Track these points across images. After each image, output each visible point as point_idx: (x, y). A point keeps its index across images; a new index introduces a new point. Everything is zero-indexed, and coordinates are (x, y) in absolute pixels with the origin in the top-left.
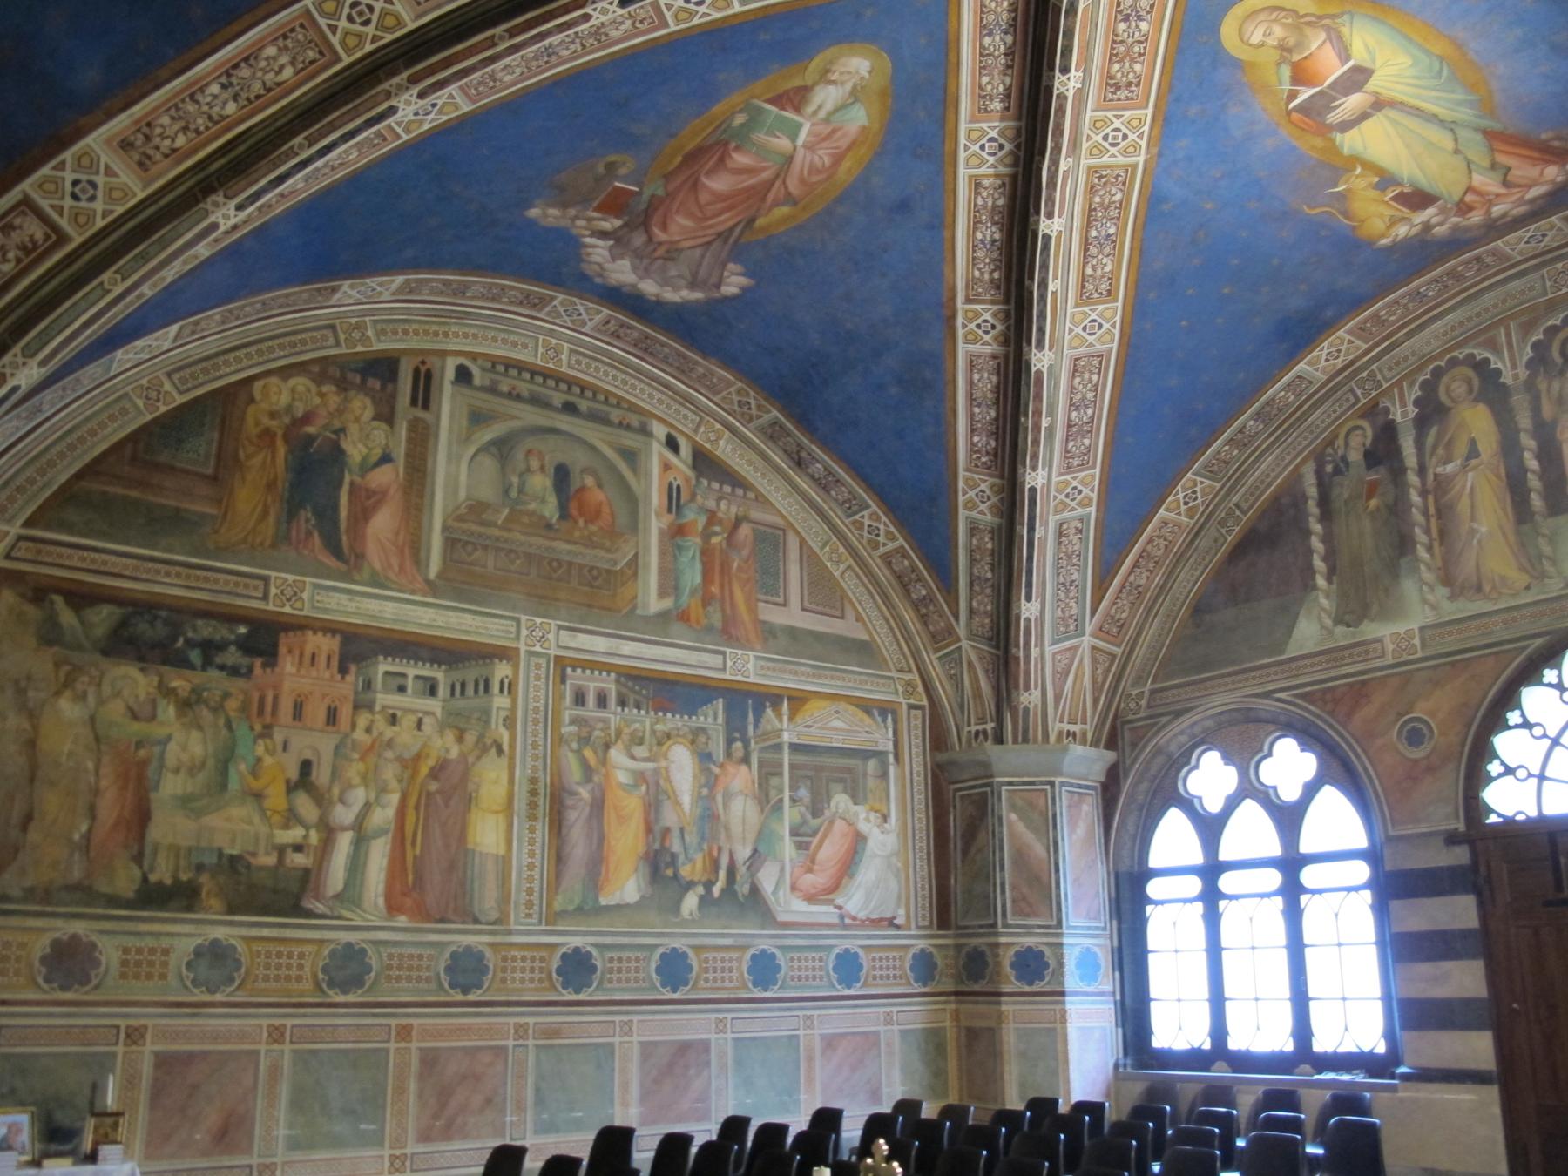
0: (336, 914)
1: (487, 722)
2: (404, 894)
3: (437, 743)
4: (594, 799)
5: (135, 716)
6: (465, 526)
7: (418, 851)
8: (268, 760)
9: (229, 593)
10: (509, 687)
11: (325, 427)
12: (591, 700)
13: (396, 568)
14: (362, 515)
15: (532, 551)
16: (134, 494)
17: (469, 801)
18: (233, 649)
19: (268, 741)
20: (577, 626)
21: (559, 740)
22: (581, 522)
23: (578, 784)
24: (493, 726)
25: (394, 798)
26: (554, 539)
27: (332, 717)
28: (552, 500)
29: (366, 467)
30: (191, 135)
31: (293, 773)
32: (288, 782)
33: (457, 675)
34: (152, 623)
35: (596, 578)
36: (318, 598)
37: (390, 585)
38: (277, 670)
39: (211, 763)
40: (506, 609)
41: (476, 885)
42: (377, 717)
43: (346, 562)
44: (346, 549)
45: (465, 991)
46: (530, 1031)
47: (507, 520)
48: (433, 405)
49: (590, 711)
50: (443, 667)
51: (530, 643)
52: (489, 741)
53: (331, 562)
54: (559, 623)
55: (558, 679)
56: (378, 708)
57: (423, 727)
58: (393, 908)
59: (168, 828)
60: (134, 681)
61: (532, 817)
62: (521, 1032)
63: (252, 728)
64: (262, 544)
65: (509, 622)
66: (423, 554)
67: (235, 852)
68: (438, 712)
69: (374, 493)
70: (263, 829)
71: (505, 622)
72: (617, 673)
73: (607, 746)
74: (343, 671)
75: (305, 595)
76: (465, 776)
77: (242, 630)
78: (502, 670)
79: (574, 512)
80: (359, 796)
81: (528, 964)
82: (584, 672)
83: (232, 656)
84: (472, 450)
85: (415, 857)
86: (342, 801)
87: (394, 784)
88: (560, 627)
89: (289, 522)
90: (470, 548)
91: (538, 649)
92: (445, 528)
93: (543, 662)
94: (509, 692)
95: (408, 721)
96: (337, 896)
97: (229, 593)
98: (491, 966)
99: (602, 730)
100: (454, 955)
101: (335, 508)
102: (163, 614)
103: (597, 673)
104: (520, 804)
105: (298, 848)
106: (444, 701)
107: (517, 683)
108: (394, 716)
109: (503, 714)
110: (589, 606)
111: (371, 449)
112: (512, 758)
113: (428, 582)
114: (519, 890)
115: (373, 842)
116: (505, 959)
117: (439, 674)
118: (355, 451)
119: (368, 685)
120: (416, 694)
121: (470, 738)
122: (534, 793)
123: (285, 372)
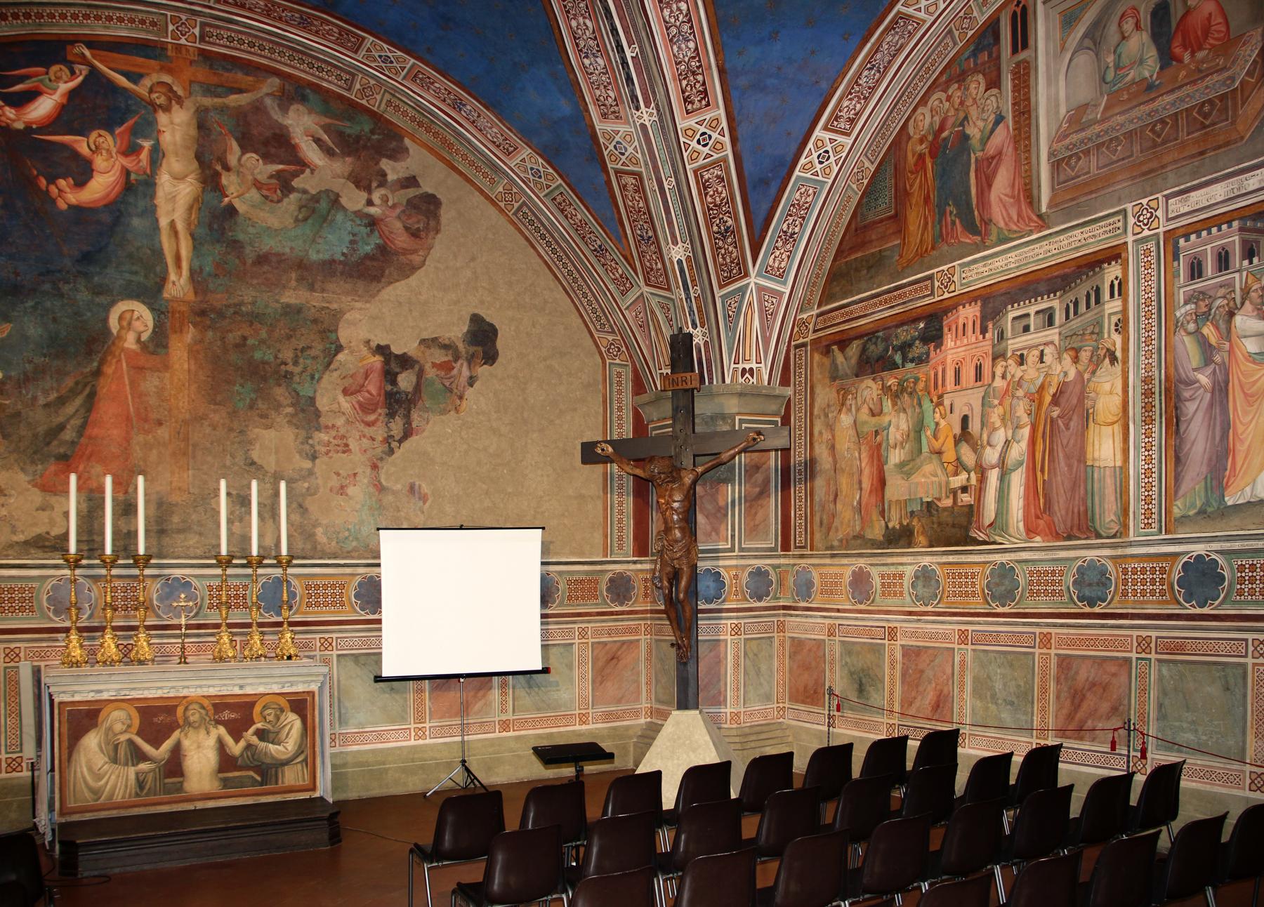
0: (992, 540)
1: (1100, 333)
2: (1037, 517)
3: (1057, 369)
4: (1215, 383)
5: (873, 415)
6: (1067, 141)
7: (1046, 478)
8: (943, 423)
9: (911, 300)
10: (1120, 288)
11: (954, 125)
12: (1209, 266)
13: (1015, 217)
14: (986, 182)
15: (1132, 127)
16: (859, 255)
17: (1086, 417)
18: (917, 342)
19: (941, 408)
20: (1189, 185)
21: (1178, 325)
22: (1187, 57)
23: (1195, 370)
24: (1106, 336)
25: (1026, 432)
26: (1153, 100)
27: (979, 375)
28: (1152, 54)
29: (985, 141)
30: (610, 87)
31: (957, 430)
32: (955, 436)
33: (1071, 296)
34: (875, 344)
35: (1206, 116)
36: (964, 275)
37: (1011, 236)
38: (943, 348)
39: (912, 435)
40: (1112, 207)
41: (1097, 499)
42: (1010, 361)
43: (979, 233)
44: (978, 223)
45: (1091, 605)
46: (1153, 645)
47: (1107, 108)
48: (1031, 42)
49: (1211, 278)
50: (1058, 294)
51: (1137, 230)
52: (1102, 352)
53: (967, 239)
54: (1166, 193)
55: (1170, 258)
56: (1009, 354)
57: (1045, 359)
58: (1031, 531)
59: (896, 489)
60: (869, 389)
61: (1148, 420)
62: (1144, 645)
63: (932, 402)
64: (926, 250)
65: (1116, 219)
66: (1035, 192)
67: (929, 500)
68: (1056, 339)
69: (993, 158)
70: (944, 478)
71: (1111, 221)
72: (1240, 219)
73: (1231, 314)
74: (984, 331)
75: (955, 279)
76: (1082, 397)
77: (922, 325)
78: (1112, 272)
79: (1178, 51)
80: (1000, 436)
81: (1148, 576)
82: (1199, 236)
83: (918, 349)
84: (1068, 56)
85: (1044, 481)
86: (989, 444)
87: (1025, 419)
88: (1167, 197)
89: (940, 222)
90: (1073, 161)
91: (1146, 233)
92: (1051, 154)
93: (1151, 245)
94: (1120, 294)
95: (1032, 357)
96: (991, 525)
97: (911, 300)
98: (1113, 578)
99: (1224, 297)
100: (1081, 570)
101: (968, 192)
102: (880, 334)
103: (1214, 230)
104: (1135, 410)
105: (964, 489)
106: (1060, 327)
107: (1127, 282)
108: (1022, 355)
109: (1114, 319)
110: (1202, 153)
111: (986, 120)
112: (1125, 361)
113: (1040, 216)
114: (1137, 500)
115: (1013, 474)
116: (1125, 572)
117: (1056, 303)
118: (973, 131)
119: (1001, 336)
120: (1037, 330)
121: (1085, 356)
122: (1148, 394)
123: (923, 101)
